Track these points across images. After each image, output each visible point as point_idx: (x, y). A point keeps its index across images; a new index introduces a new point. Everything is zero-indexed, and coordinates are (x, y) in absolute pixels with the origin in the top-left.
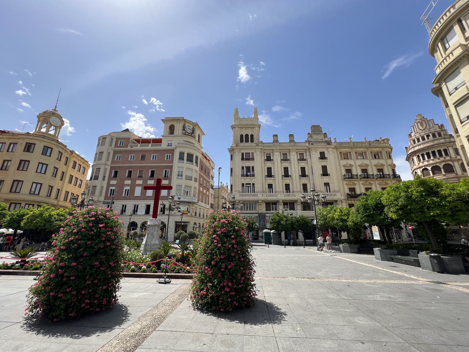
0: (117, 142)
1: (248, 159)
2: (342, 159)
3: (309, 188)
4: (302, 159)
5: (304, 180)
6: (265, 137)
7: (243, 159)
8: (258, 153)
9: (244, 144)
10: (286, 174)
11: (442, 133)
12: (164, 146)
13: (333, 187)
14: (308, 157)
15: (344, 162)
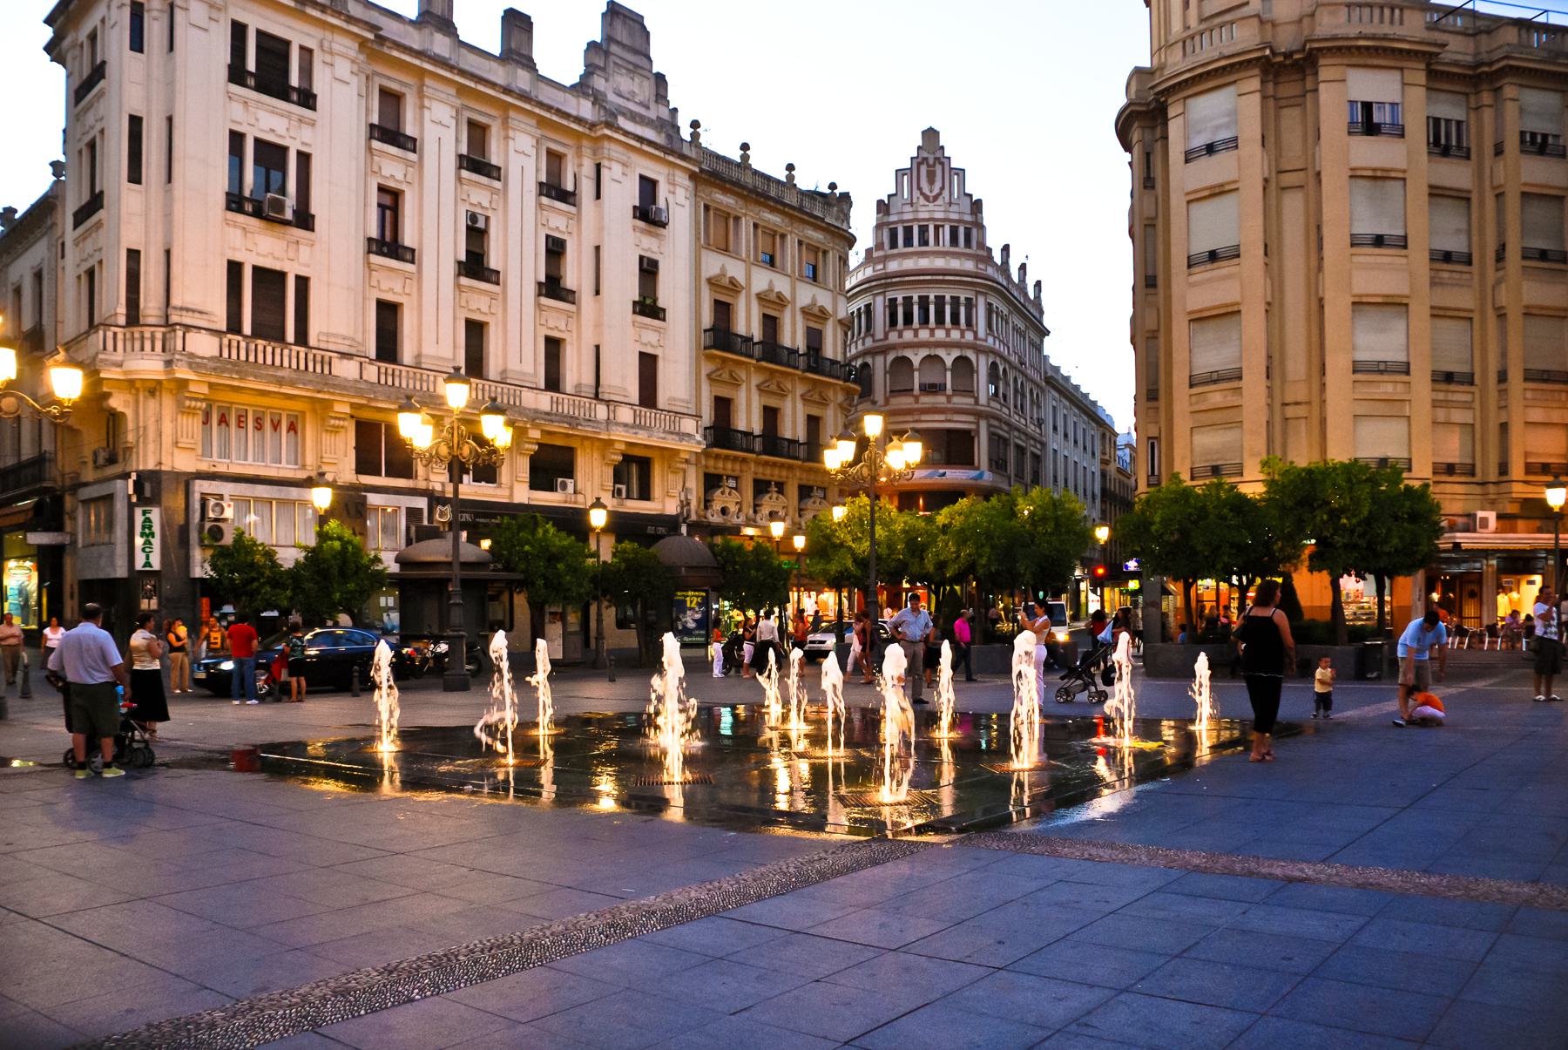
2: (708, 246)
3: (576, 370)
4: (554, 190)
7: (237, 74)
8: (343, 68)
10: (475, 265)
11: (974, 231)
14: (587, 188)
15: (713, 264)
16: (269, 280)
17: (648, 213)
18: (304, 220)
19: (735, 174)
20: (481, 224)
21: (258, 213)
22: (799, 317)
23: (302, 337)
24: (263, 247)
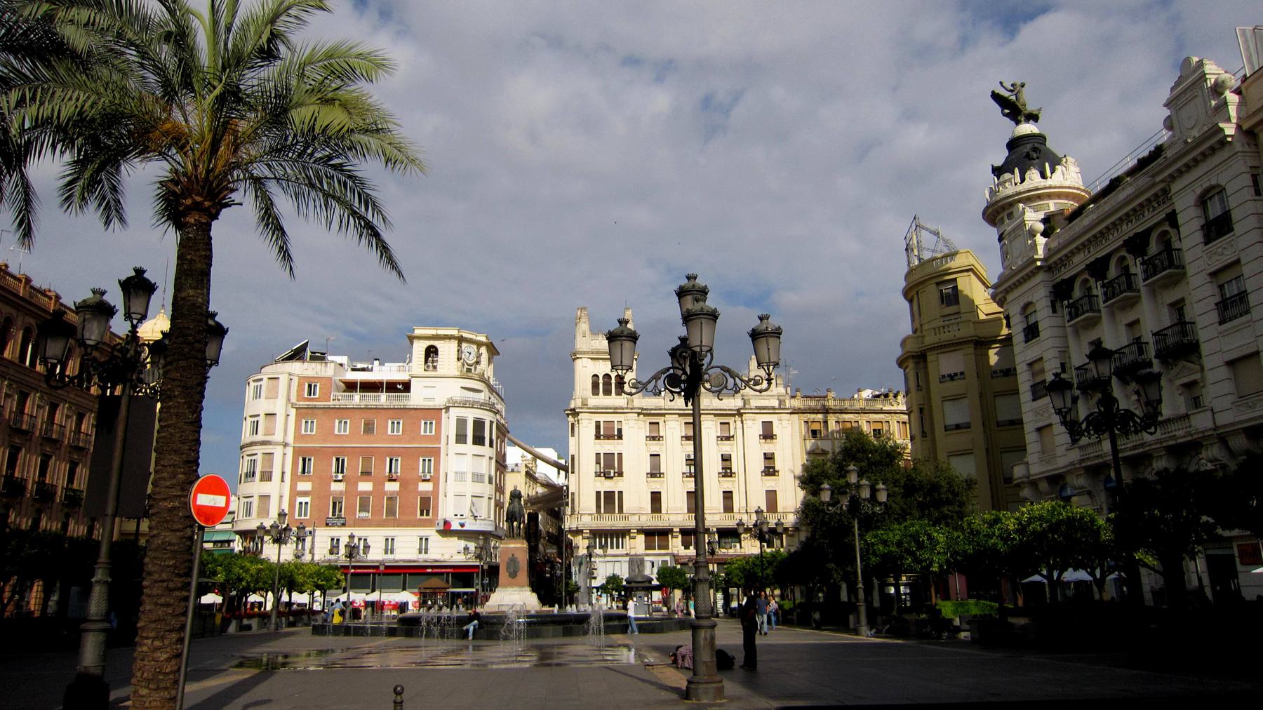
1: (609, 437)
3: (738, 502)
7: (598, 437)
12: (417, 398)
14: (739, 432)
16: (609, 496)
17: (768, 435)
18: (620, 474)
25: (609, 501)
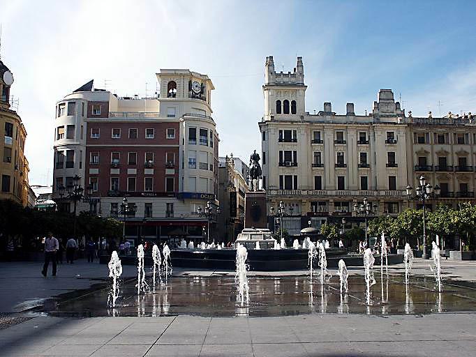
0: (89, 107)
5: (364, 172)
6: (312, 104)
8: (303, 132)
9: (283, 116)
10: (341, 163)
13: (401, 182)
15: (418, 147)
16: (288, 178)
17: (390, 139)
18: (296, 165)
19: (429, 122)
20: (341, 154)
21: (285, 166)
22: (455, 155)
23: (296, 188)
24: (286, 172)
25: (289, 182)
